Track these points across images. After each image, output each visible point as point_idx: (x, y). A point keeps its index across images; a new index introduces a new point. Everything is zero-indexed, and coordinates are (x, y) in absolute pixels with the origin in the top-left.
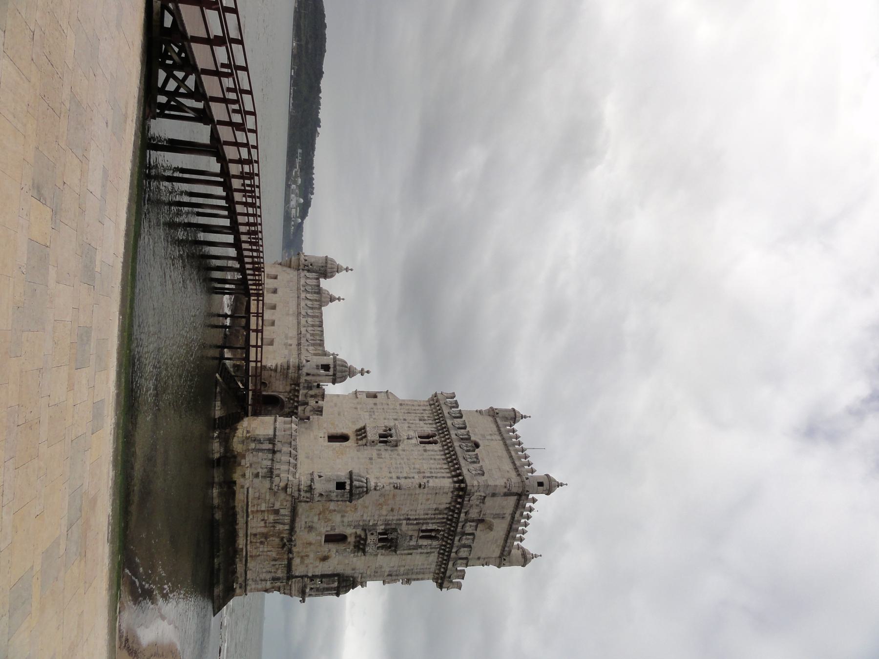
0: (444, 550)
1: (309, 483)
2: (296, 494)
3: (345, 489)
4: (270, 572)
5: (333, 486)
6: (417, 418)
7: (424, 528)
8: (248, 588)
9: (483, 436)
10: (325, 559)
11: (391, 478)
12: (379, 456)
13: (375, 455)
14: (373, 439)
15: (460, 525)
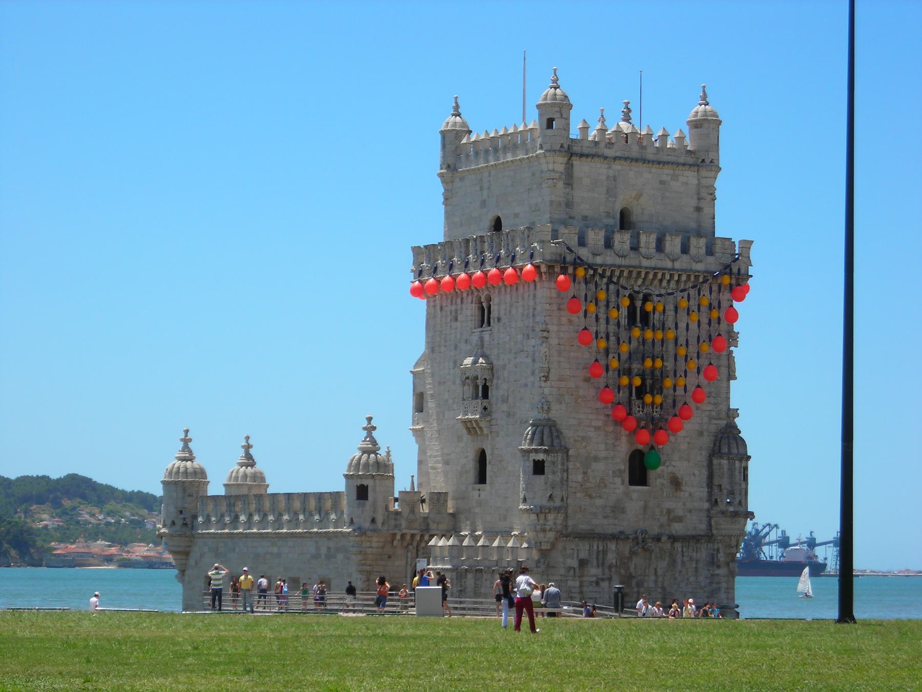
0: (669, 281)
1: (533, 517)
2: (551, 535)
3: (543, 461)
4: (696, 570)
5: (540, 479)
6: (454, 324)
7: (624, 322)
8: (725, 602)
9: (483, 204)
10: (676, 483)
11: (533, 383)
12: (505, 400)
13: (504, 407)
14: (480, 409)
15: (618, 261)
